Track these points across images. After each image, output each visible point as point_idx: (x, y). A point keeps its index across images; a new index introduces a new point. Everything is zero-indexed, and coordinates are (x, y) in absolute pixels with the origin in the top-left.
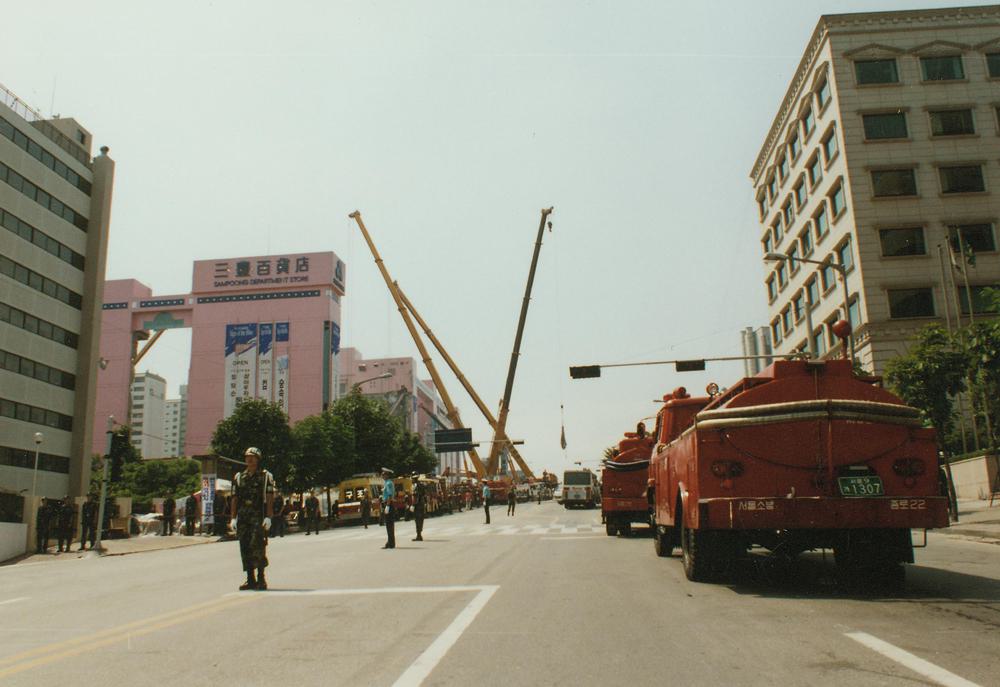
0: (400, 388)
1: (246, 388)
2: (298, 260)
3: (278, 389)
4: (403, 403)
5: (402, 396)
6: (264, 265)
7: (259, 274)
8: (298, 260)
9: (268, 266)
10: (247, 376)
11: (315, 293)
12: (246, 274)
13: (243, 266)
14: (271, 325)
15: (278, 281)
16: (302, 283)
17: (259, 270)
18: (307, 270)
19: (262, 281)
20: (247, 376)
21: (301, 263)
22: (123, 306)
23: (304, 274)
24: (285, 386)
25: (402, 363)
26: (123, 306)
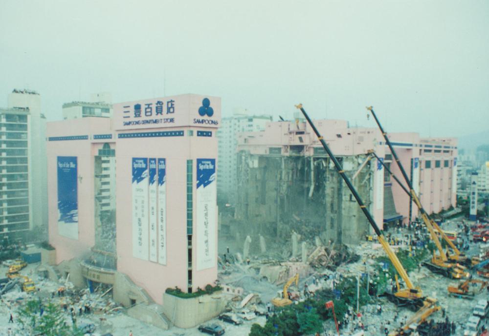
0: (366, 153)
1: (143, 211)
2: (168, 102)
3: (160, 216)
4: (369, 163)
5: (368, 158)
6: (148, 108)
7: (146, 115)
8: (168, 102)
9: (151, 108)
10: (143, 202)
11: (180, 134)
12: (139, 116)
13: (138, 107)
14: (155, 159)
15: (156, 122)
16: (171, 124)
17: (146, 112)
18: (173, 112)
19: (147, 122)
20: (143, 202)
21: (170, 106)
22: (85, 138)
23: (170, 116)
24: (164, 213)
25: (369, 132)
26: (85, 138)
